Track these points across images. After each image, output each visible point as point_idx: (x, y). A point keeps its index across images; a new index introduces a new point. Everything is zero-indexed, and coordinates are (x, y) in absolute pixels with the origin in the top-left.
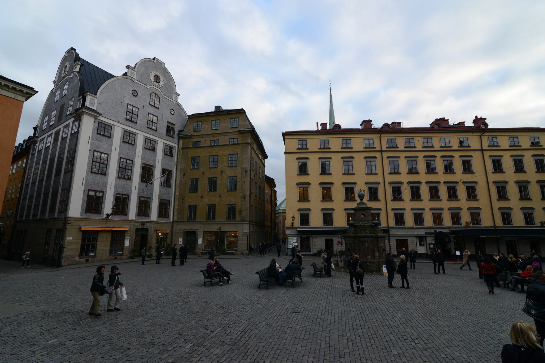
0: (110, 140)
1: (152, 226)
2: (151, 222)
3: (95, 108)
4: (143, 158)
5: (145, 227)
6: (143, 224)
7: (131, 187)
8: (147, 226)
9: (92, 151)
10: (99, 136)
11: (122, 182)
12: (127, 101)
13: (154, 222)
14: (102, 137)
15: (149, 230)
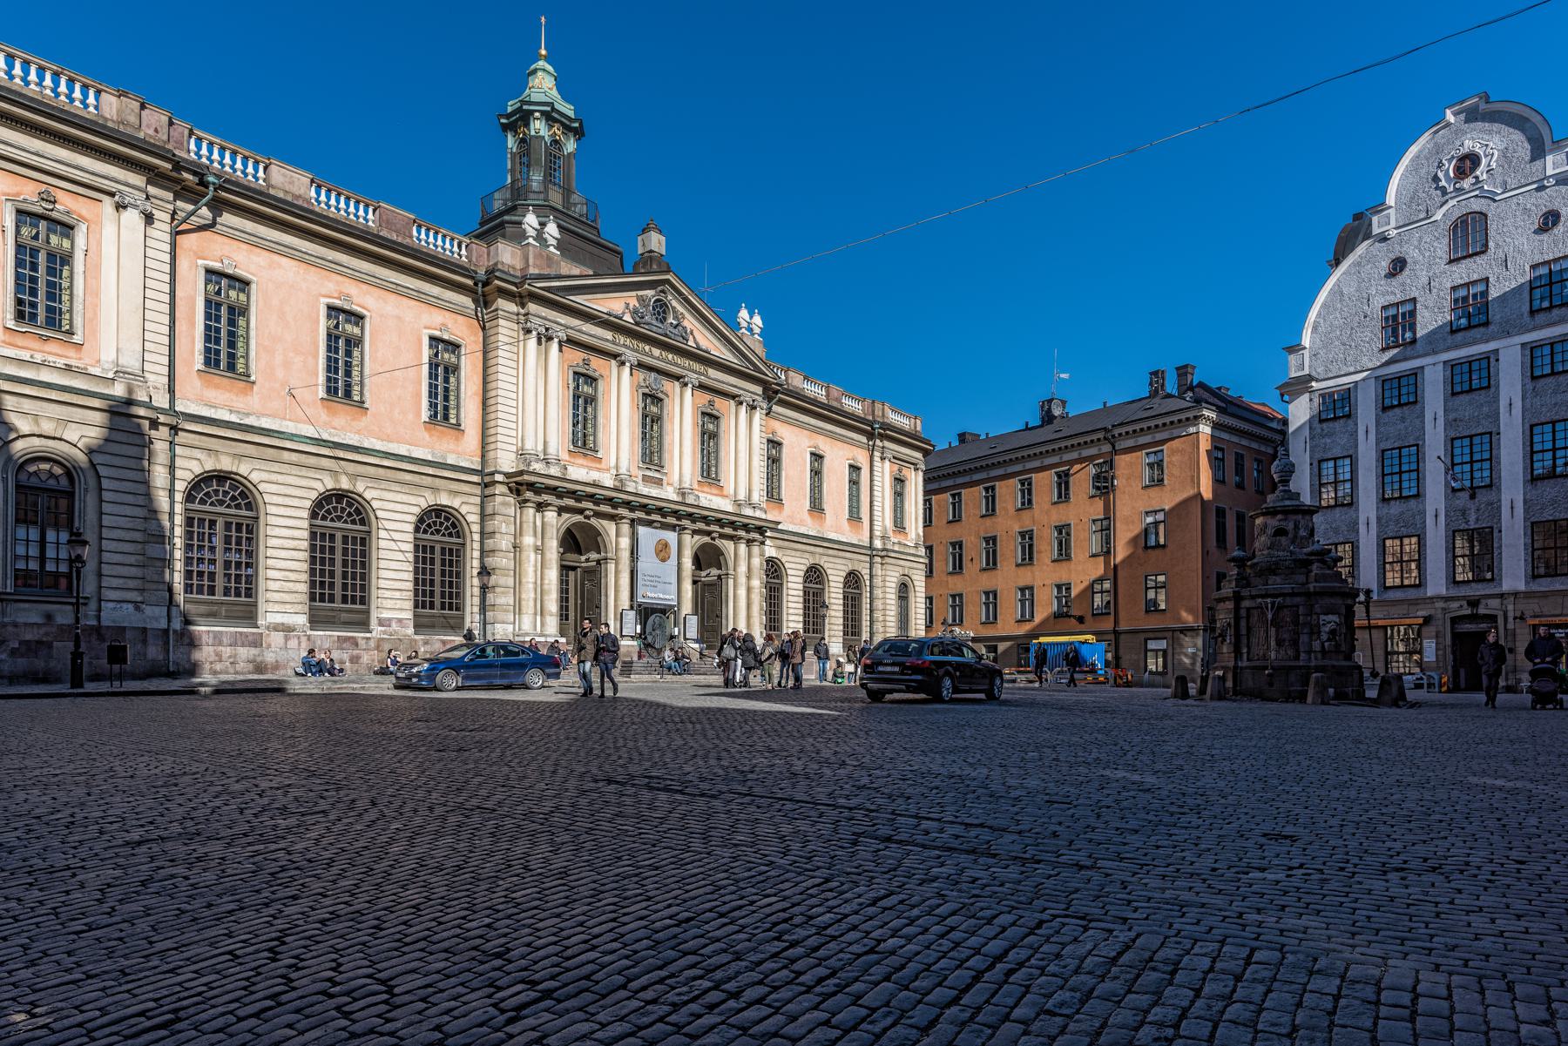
0: (1350, 422)
1: (1510, 607)
2: (1502, 596)
3: (1306, 371)
4: (1448, 424)
5: (1482, 611)
6: (1473, 603)
7: (1423, 513)
8: (1490, 607)
9: (1315, 464)
10: (1325, 425)
11: (1395, 508)
12: (1379, 302)
13: (1516, 594)
14: (1331, 424)
15: (1500, 621)
